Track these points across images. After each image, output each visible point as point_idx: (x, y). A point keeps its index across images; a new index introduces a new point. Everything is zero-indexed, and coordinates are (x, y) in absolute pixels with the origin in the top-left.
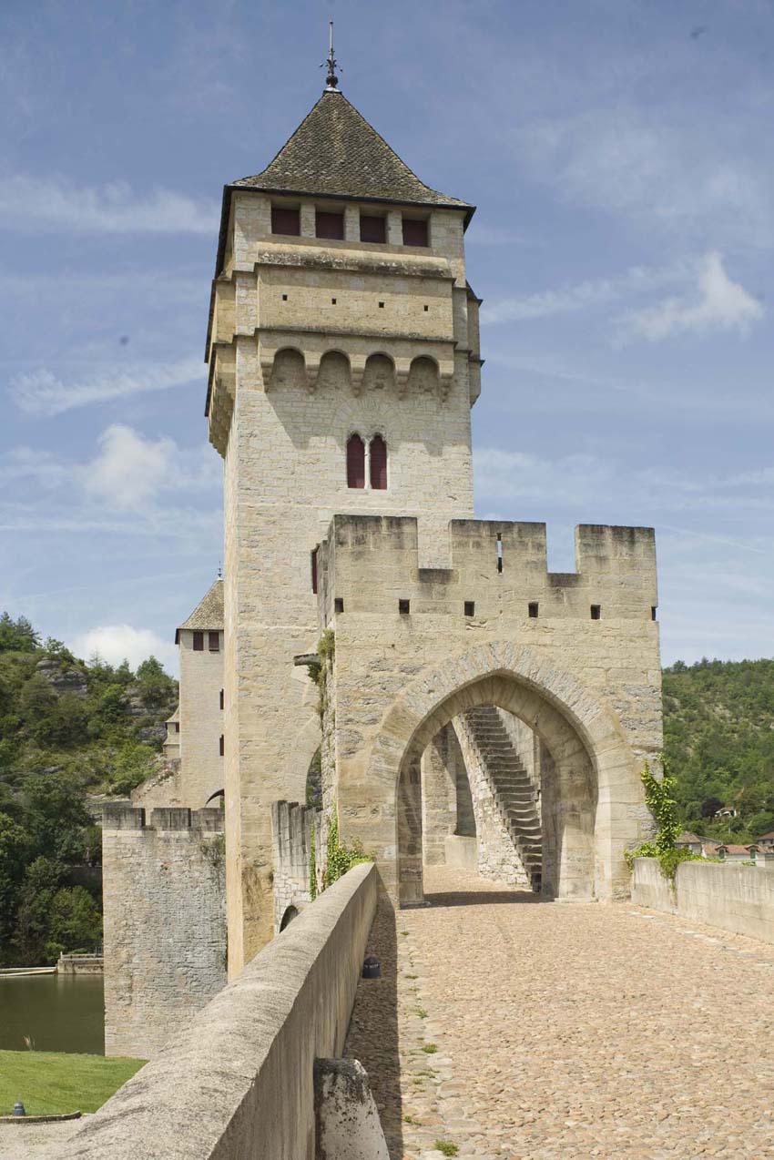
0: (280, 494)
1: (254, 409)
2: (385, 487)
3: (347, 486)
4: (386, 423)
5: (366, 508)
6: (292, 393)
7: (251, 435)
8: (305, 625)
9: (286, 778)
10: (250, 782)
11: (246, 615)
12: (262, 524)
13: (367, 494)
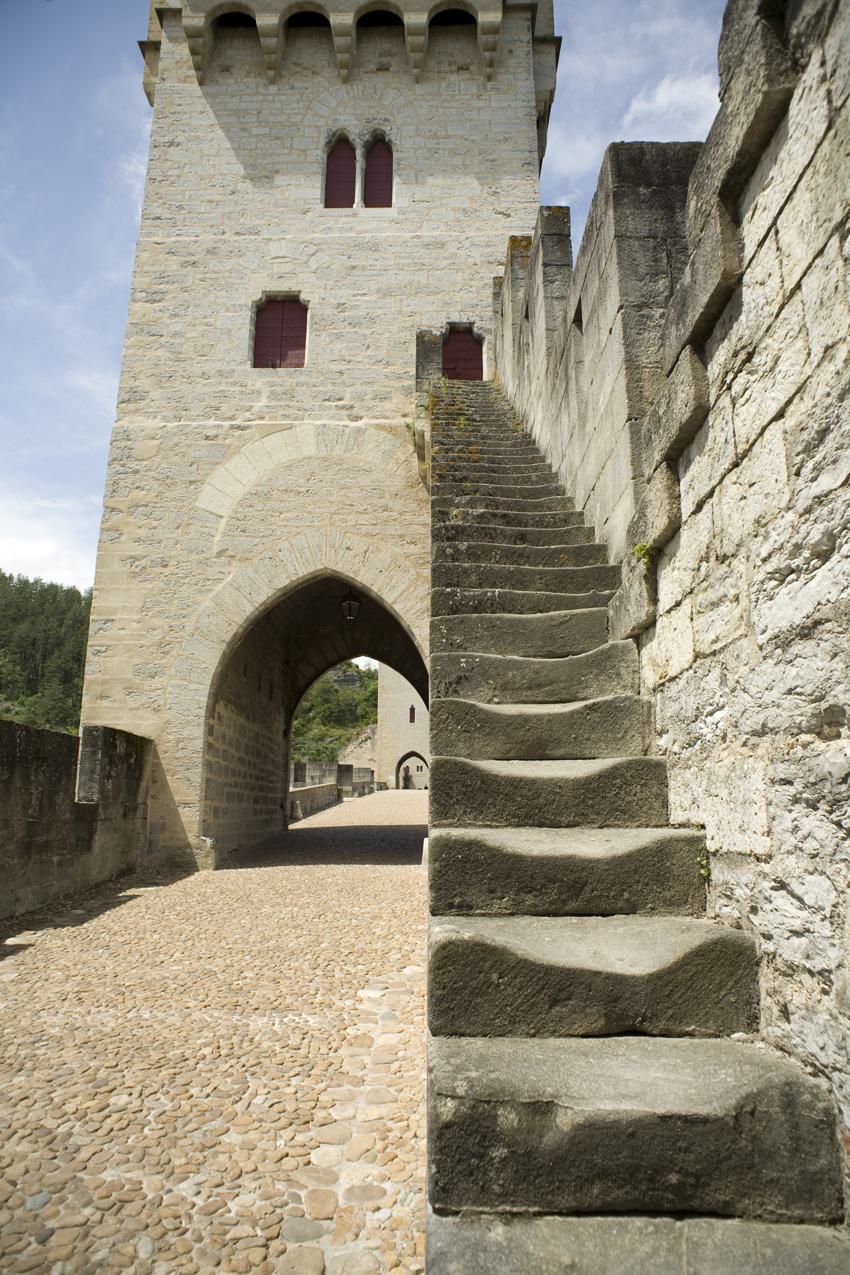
0: (213, 222)
1: (179, 109)
2: (386, 202)
3: (322, 206)
4: (392, 114)
5: (352, 234)
6: (245, 87)
7: (171, 144)
8: (232, 418)
9: (169, 689)
10: (102, 697)
11: (131, 406)
12: (175, 267)
13: (355, 215)
